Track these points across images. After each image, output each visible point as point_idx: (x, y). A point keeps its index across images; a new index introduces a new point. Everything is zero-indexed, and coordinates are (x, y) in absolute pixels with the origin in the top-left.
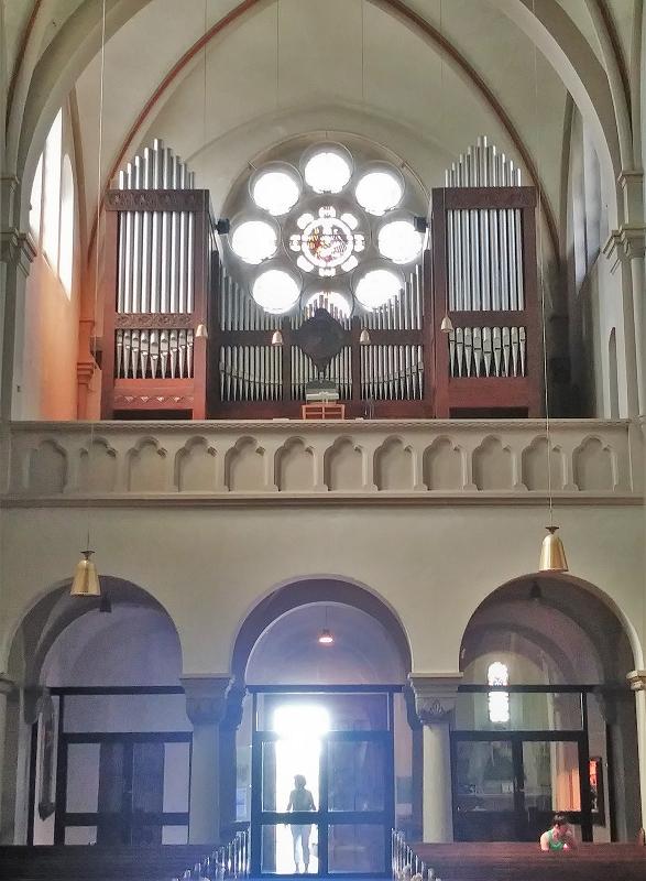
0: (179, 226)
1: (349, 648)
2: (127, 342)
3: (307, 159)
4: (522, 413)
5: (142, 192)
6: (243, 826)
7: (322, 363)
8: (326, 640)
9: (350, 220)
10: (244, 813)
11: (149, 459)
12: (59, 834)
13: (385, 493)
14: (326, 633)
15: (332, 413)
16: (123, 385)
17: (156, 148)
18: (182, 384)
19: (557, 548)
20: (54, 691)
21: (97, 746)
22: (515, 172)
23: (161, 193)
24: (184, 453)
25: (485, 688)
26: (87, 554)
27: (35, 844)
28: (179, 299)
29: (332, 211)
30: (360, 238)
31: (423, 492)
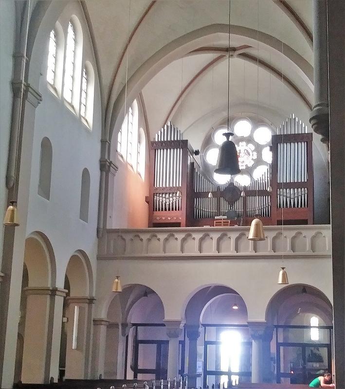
0: (179, 152)
1: (226, 310)
2: (158, 198)
3: (235, 123)
4: (305, 222)
5: (164, 142)
6: (199, 375)
7: (231, 203)
8: (235, 308)
9: (251, 147)
10: (200, 370)
11: (154, 242)
12: (135, 376)
13: (239, 254)
14: (235, 305)
15: (226, 224)
16: (156, 213)
17: (169, 125)
18: (178, 213)
19: (284, 275)
20: (134, 325)
21: (155, 346)
22: (305, 127)
23: (171, 142)
24: (166, 240)
25: (309, 327)
26: (118, 277)
27: (127, 379)
28: (177, 181)
29: (244, 143)
30: (255, 154)
31: (253, 253)
